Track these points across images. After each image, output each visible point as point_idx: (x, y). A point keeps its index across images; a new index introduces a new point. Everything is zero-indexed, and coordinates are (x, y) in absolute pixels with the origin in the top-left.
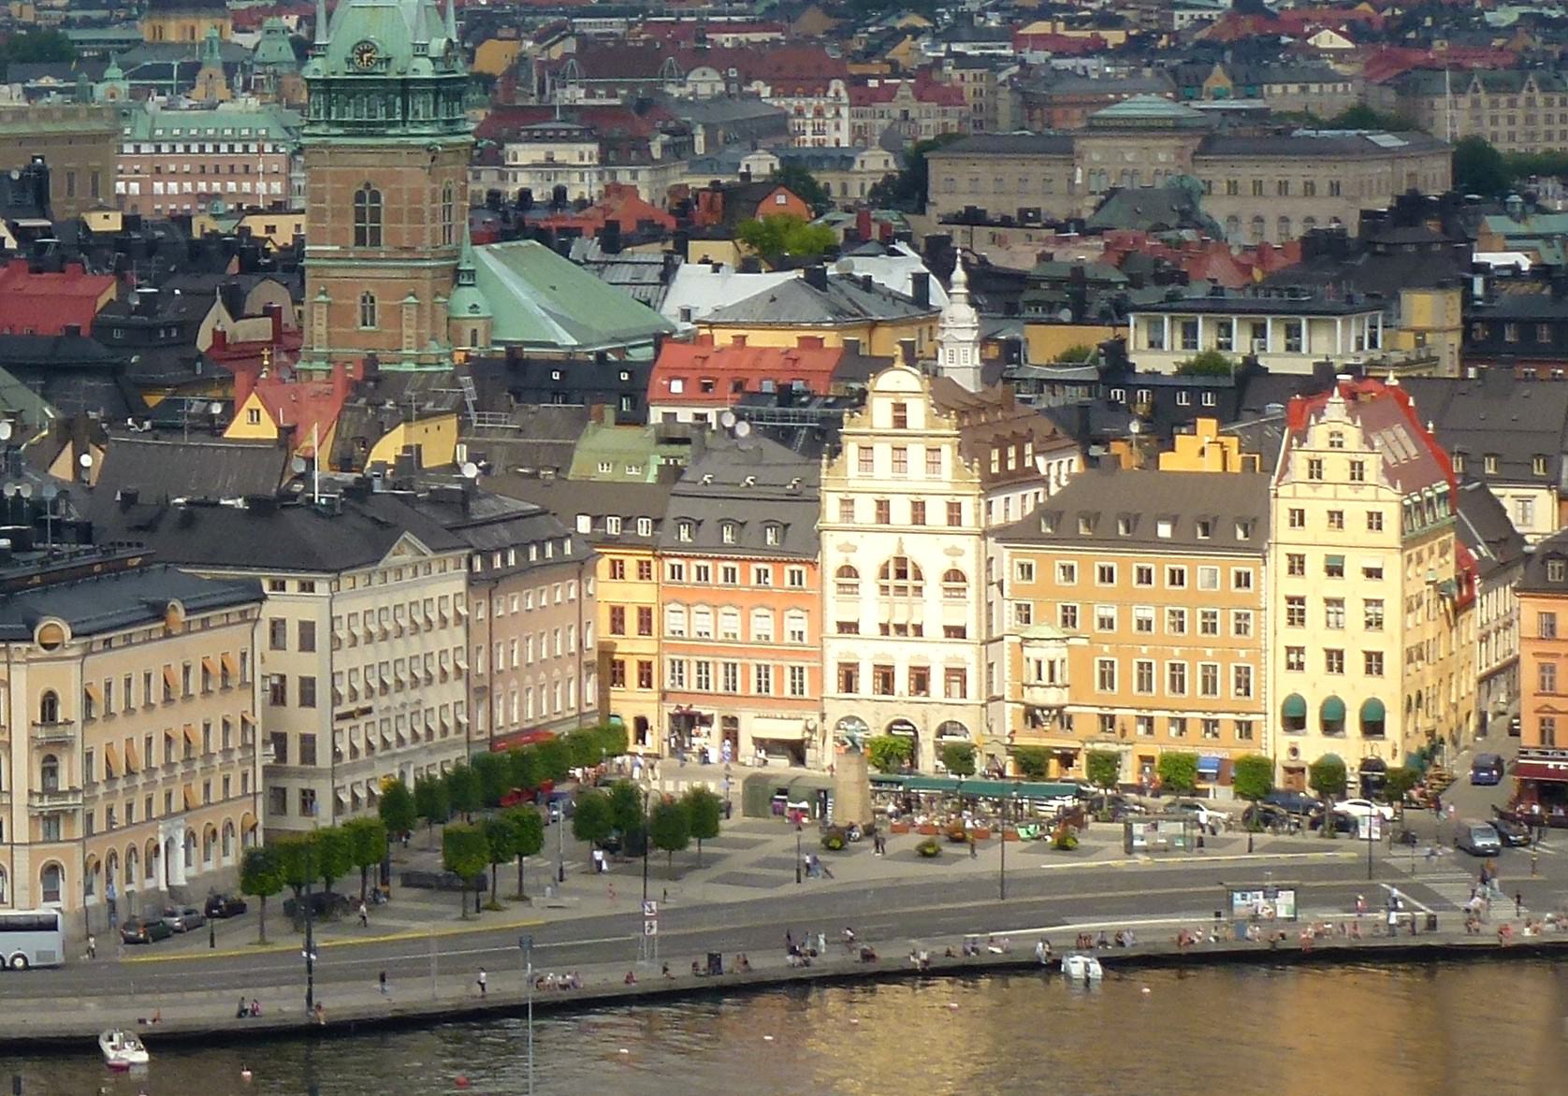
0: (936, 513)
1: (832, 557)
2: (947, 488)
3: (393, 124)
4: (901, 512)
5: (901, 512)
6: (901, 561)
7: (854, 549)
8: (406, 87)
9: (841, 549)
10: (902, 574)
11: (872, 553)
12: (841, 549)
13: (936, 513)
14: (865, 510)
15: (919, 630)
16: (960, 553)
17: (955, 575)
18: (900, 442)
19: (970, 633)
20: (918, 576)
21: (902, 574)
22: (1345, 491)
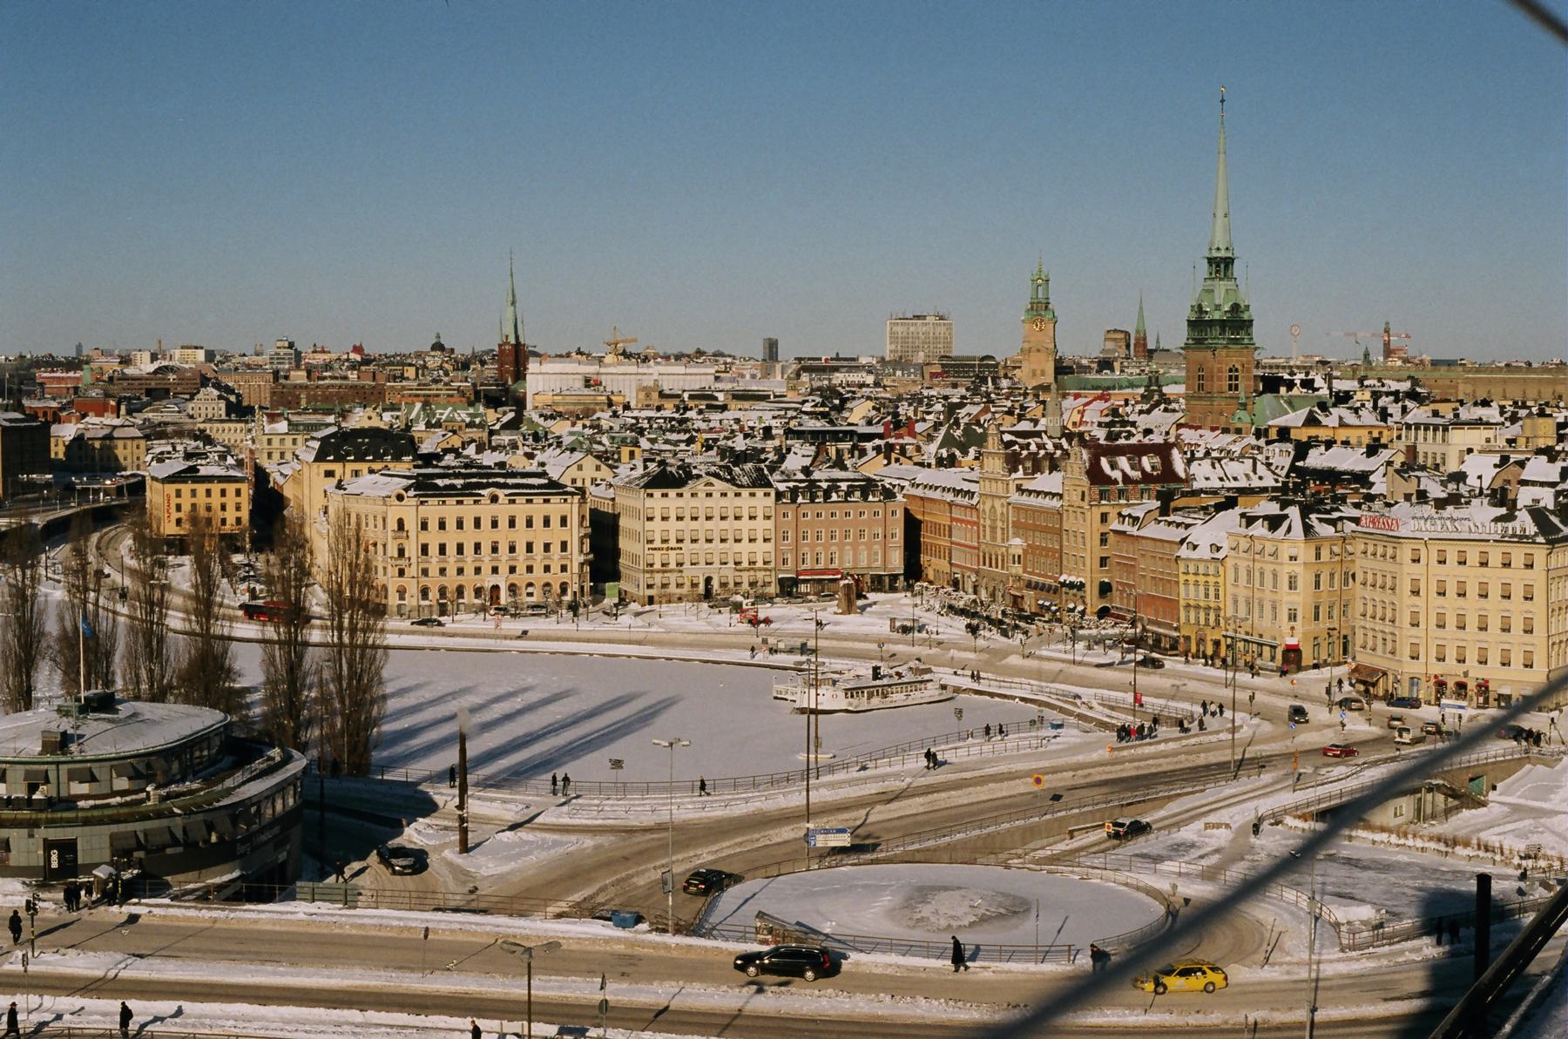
8: (1212, 323)
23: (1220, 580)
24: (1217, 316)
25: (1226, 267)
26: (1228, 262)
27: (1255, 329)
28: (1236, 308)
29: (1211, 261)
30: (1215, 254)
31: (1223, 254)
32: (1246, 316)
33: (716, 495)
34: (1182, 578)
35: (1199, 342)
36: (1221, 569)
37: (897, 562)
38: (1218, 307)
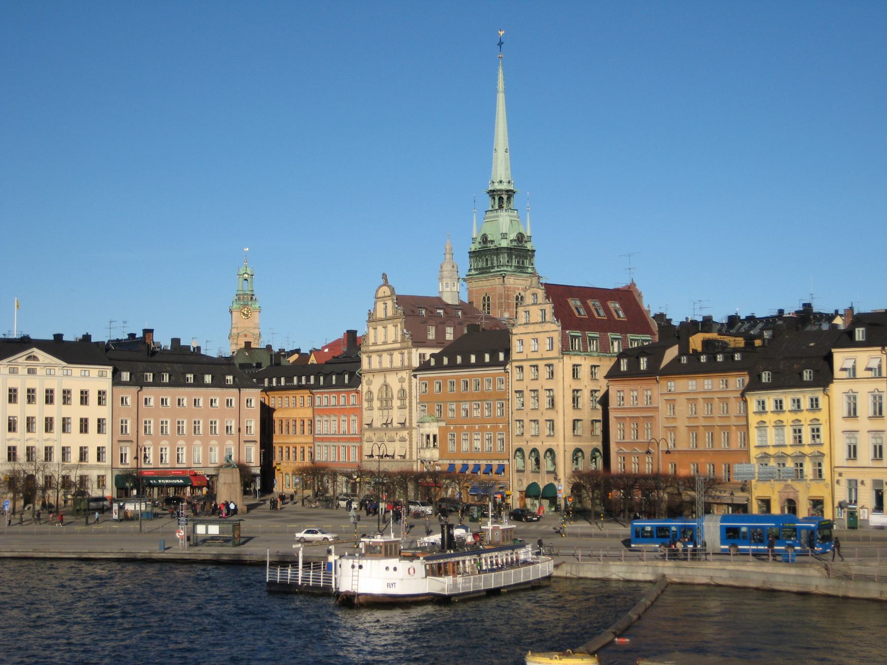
1: (364, 387)
2: (398, 345)
3: (493, 267)
8: (498, 251)
22: (538, 328)
23: (822, 416)
24: (504, 244)
25: (509, 198)
26: (510, 193)
27: (536, 260)
28: (520, 238)
29: (492, 193)
30: (498, 186)
31: (505, 186)
32: (529, 246)
33: (40, 371)
34: (754, 420)
35: (483, 271)
36: (823, 402)
37: (540, 320)
38: (504, 236)
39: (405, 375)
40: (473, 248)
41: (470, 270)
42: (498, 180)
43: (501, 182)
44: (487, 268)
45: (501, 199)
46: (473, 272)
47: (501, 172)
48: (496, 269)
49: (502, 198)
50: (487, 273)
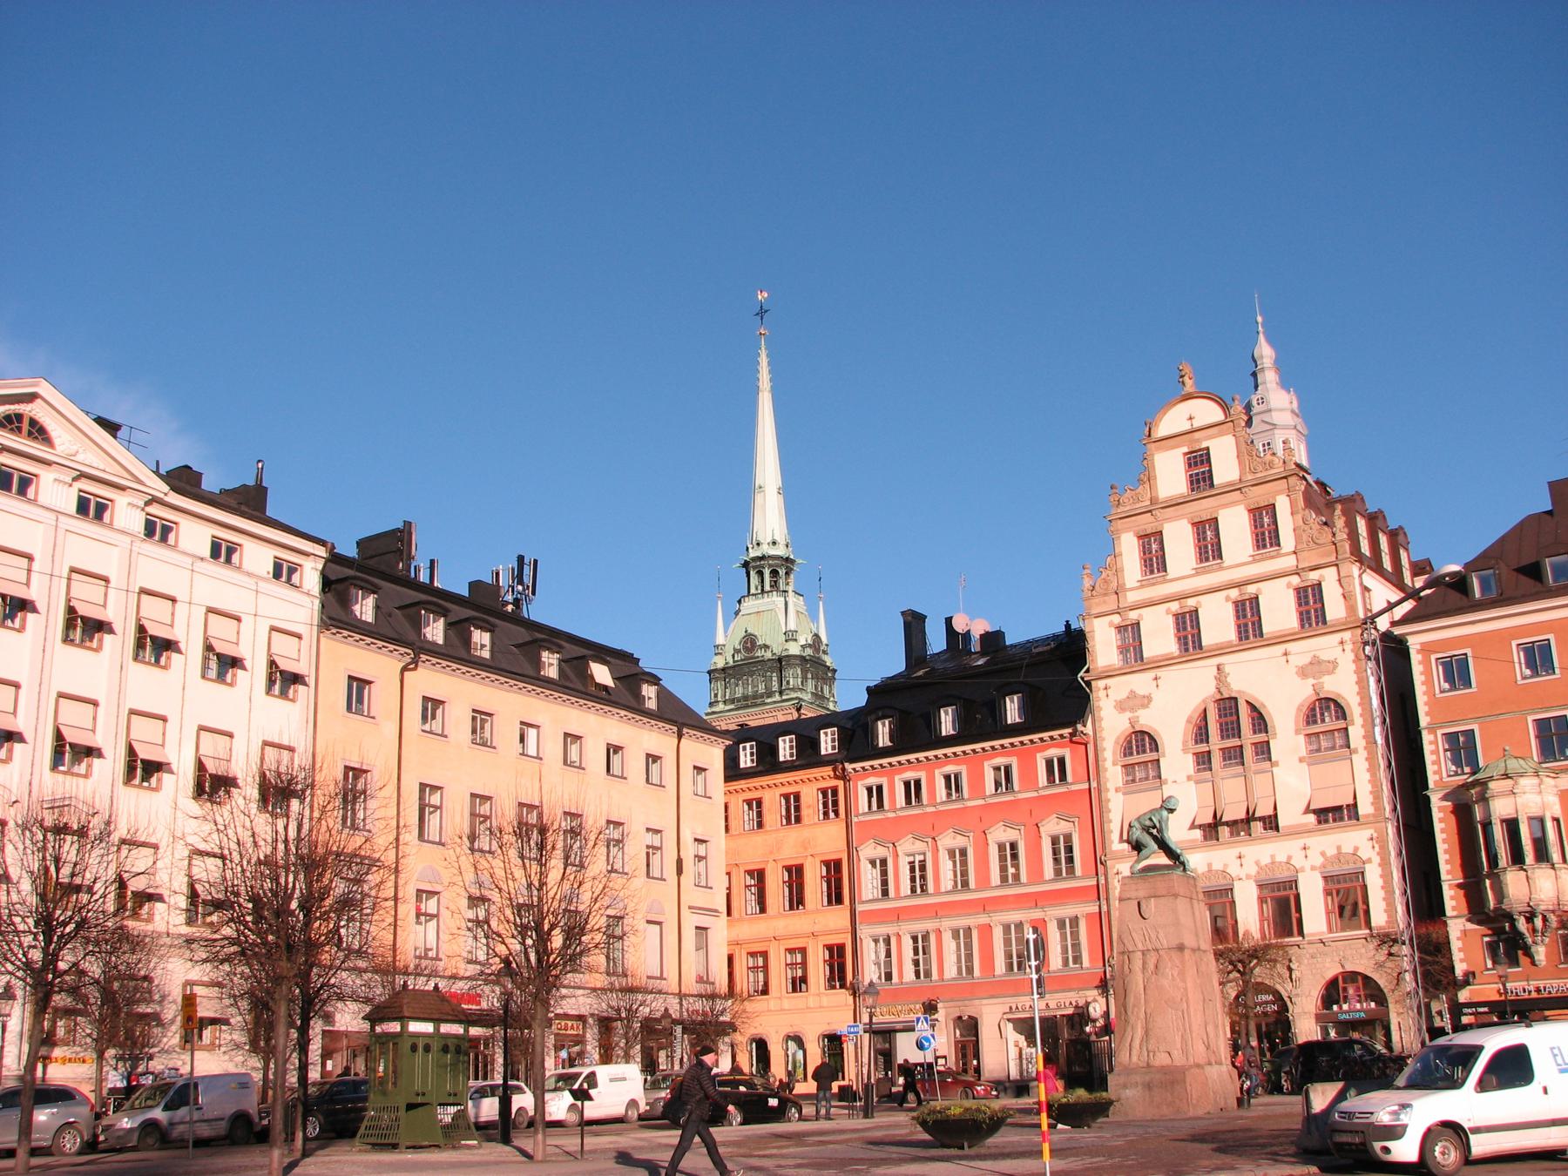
0: (1279, 610)
2: (1290, 562)
3: (770, 694)
4: (1218, 622)
5: (1218, 622)
6: (1228, 706)
7: (1146, 701)
8: (781, 663)
9: (1121, 706)
10: (1231, 728)
11: (1174, 700)
12: (1121, 706)
13: (1279, 610)
14: (1159, 637)
15: (1271, 823)
16: (1333, 666)
17: (1324, 709)
18: (1203, 508)
19: (1365, 808)
20: (1260, 722)
21: (1231, 728)
24: (794, 649)
31: (780, 551)
38: (790, 636)
39: (1326, 646)
40: (720, 662)
41: (711, 705)
42: (769, 540)
43: (774, 543)
44: (755, 696)
45: (774, 573)
46: (721, 707)
47: (770, 525)
48: (777, 697)
49: (769, 572)
50: (756, 705)
